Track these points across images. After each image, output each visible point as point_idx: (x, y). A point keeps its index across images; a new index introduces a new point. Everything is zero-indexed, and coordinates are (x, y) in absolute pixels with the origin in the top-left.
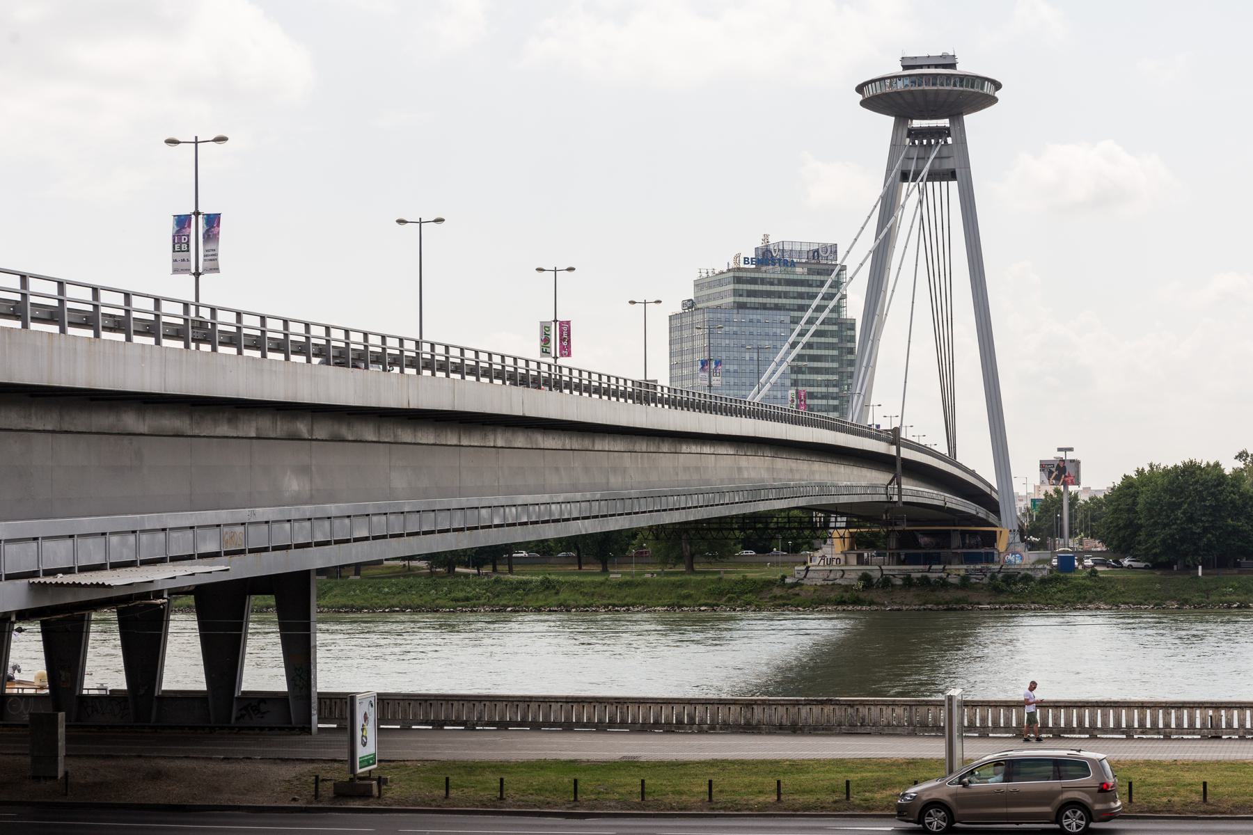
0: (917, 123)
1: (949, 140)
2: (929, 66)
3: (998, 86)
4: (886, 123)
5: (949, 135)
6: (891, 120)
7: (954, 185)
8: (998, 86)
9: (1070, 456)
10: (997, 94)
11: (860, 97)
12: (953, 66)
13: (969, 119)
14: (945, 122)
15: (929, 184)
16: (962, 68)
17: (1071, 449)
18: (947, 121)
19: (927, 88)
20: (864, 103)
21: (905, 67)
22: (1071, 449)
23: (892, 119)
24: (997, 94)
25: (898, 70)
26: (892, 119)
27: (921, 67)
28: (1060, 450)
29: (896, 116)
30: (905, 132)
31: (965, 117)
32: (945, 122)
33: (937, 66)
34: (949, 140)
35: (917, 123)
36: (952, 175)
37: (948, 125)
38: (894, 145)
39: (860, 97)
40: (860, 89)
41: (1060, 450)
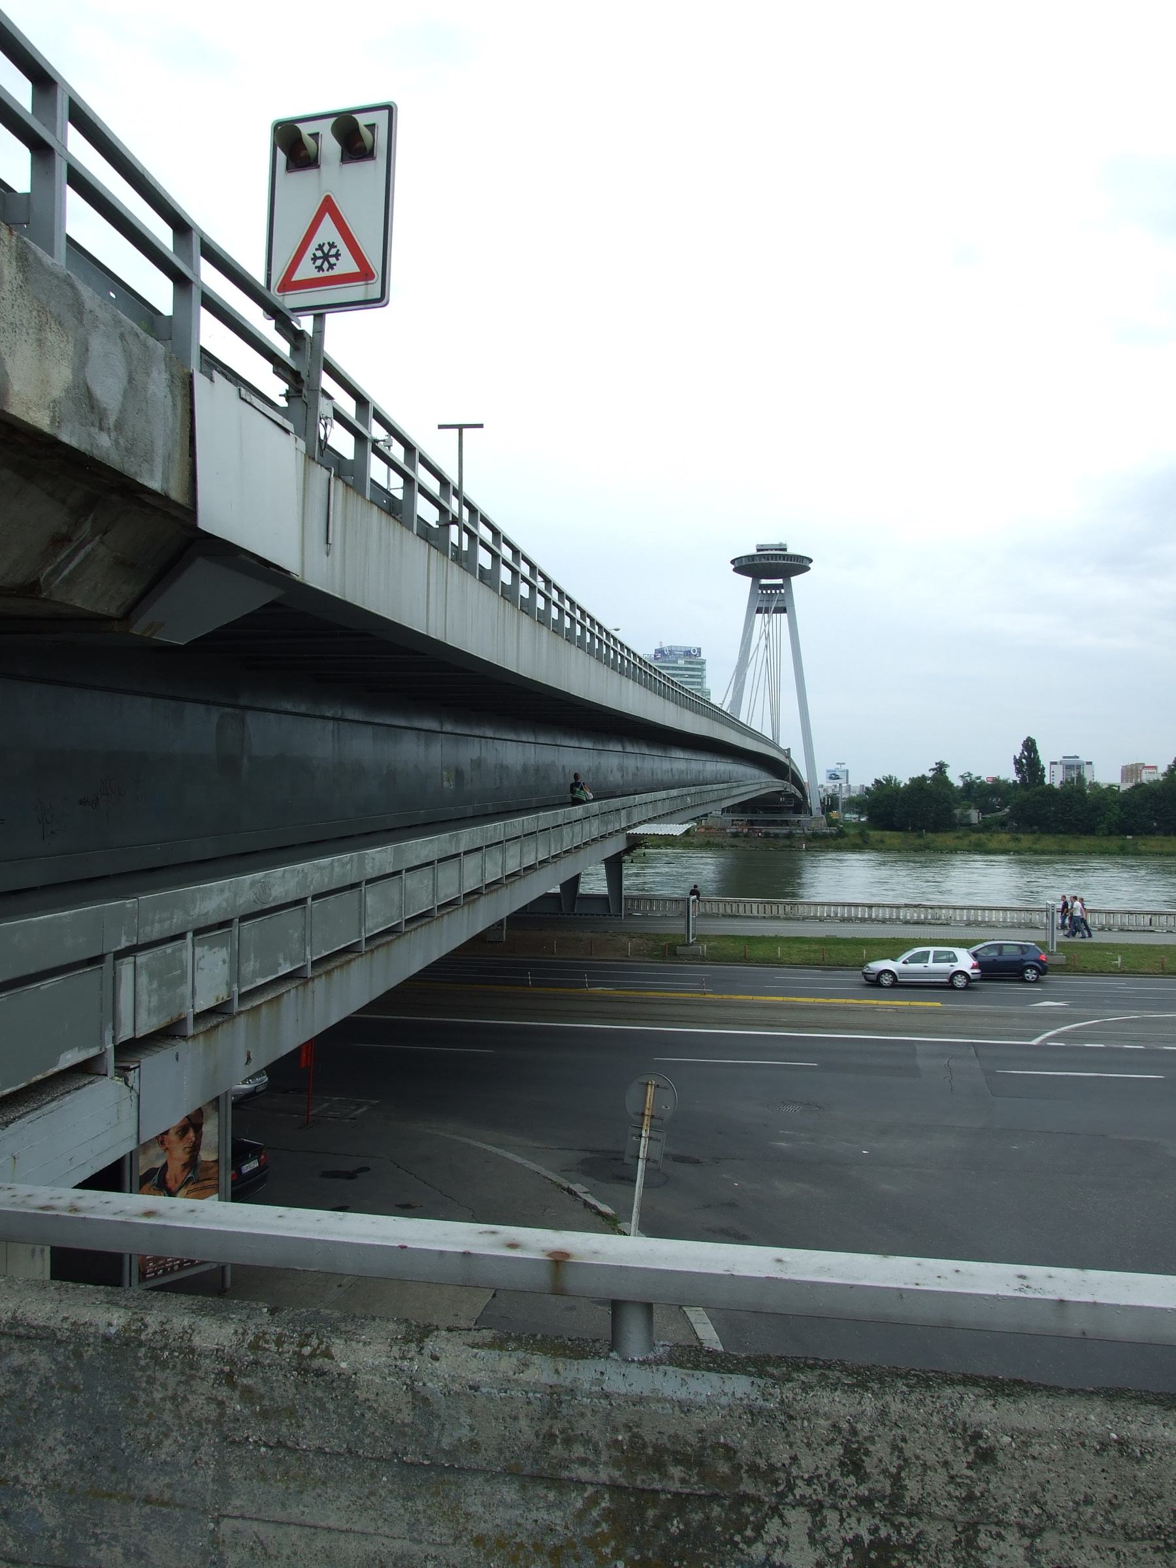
0: (764, 582)
1: (783, 591)
2: (772, 550)
3: (811, 561)
4: (747, 581)
6: (750, 579)
7: (784, 615)
8: (811, 561)
9: (844, 767)
10: (810, 565)
11: (733, 567)
12: (785, 550)
13: (793, 579)
14: (780, 581)
15: (774, 615)
16: (790, 551)
17: (844, 764)
18: (781, 580)
20: (735, 570)
21: (758, 550)
22: (844, 764)
23: (750, 579)
24: (810, 565)
25: (753, 551)
27: (767, 550)
28: (838, 764)
31: (792, 578)
32: (780, 581)
33: (776, 550)
34: (783, 591)
35: (764, 582)
36: (784, 610)
37: (782, 582)
39: (733, 567)
40: (733, 562)
41: (838, 764)
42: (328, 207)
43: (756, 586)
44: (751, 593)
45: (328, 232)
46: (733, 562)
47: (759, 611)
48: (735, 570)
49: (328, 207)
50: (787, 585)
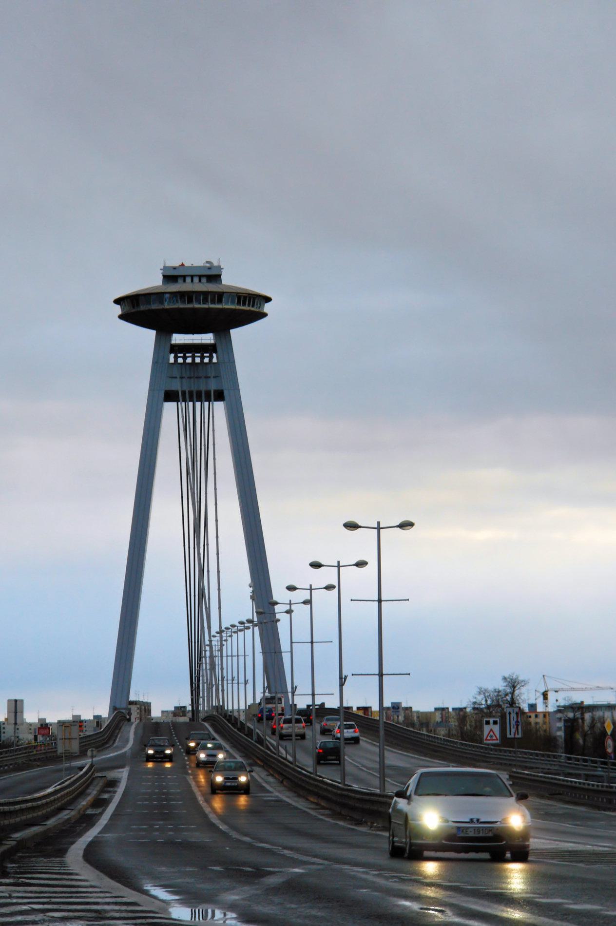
0: (178, 339)
5: (216, 352)
6: (151, 334)
7: (219, 408)
8: (268, 299)
10: (267, 308)
11: (118, 310)
13: (235, 333)
14: (207, 338)
19: (197, 306)
26: (153, 333)
29: (156, 330)
30: (168, 348)
32: (207, 338)
34: (215, 360)
35: (178, 339)
36: (220, 396)
37: (212, 342)
38: (158, 362)
40: (117, 301)
42: (491, 730)
43: (163, 347)
44: (155, 363)
45: (491, 733)
46: (117, 301)
47: (170, 396)
48: (121, 317)
49: (491, 730)
50: (223, 345)
